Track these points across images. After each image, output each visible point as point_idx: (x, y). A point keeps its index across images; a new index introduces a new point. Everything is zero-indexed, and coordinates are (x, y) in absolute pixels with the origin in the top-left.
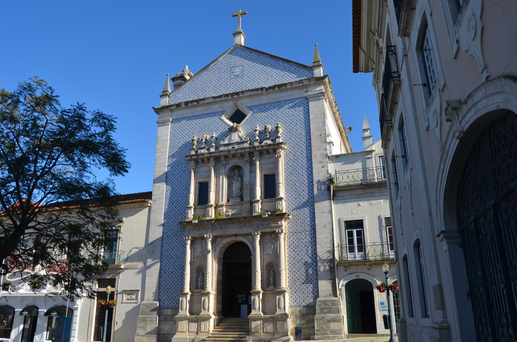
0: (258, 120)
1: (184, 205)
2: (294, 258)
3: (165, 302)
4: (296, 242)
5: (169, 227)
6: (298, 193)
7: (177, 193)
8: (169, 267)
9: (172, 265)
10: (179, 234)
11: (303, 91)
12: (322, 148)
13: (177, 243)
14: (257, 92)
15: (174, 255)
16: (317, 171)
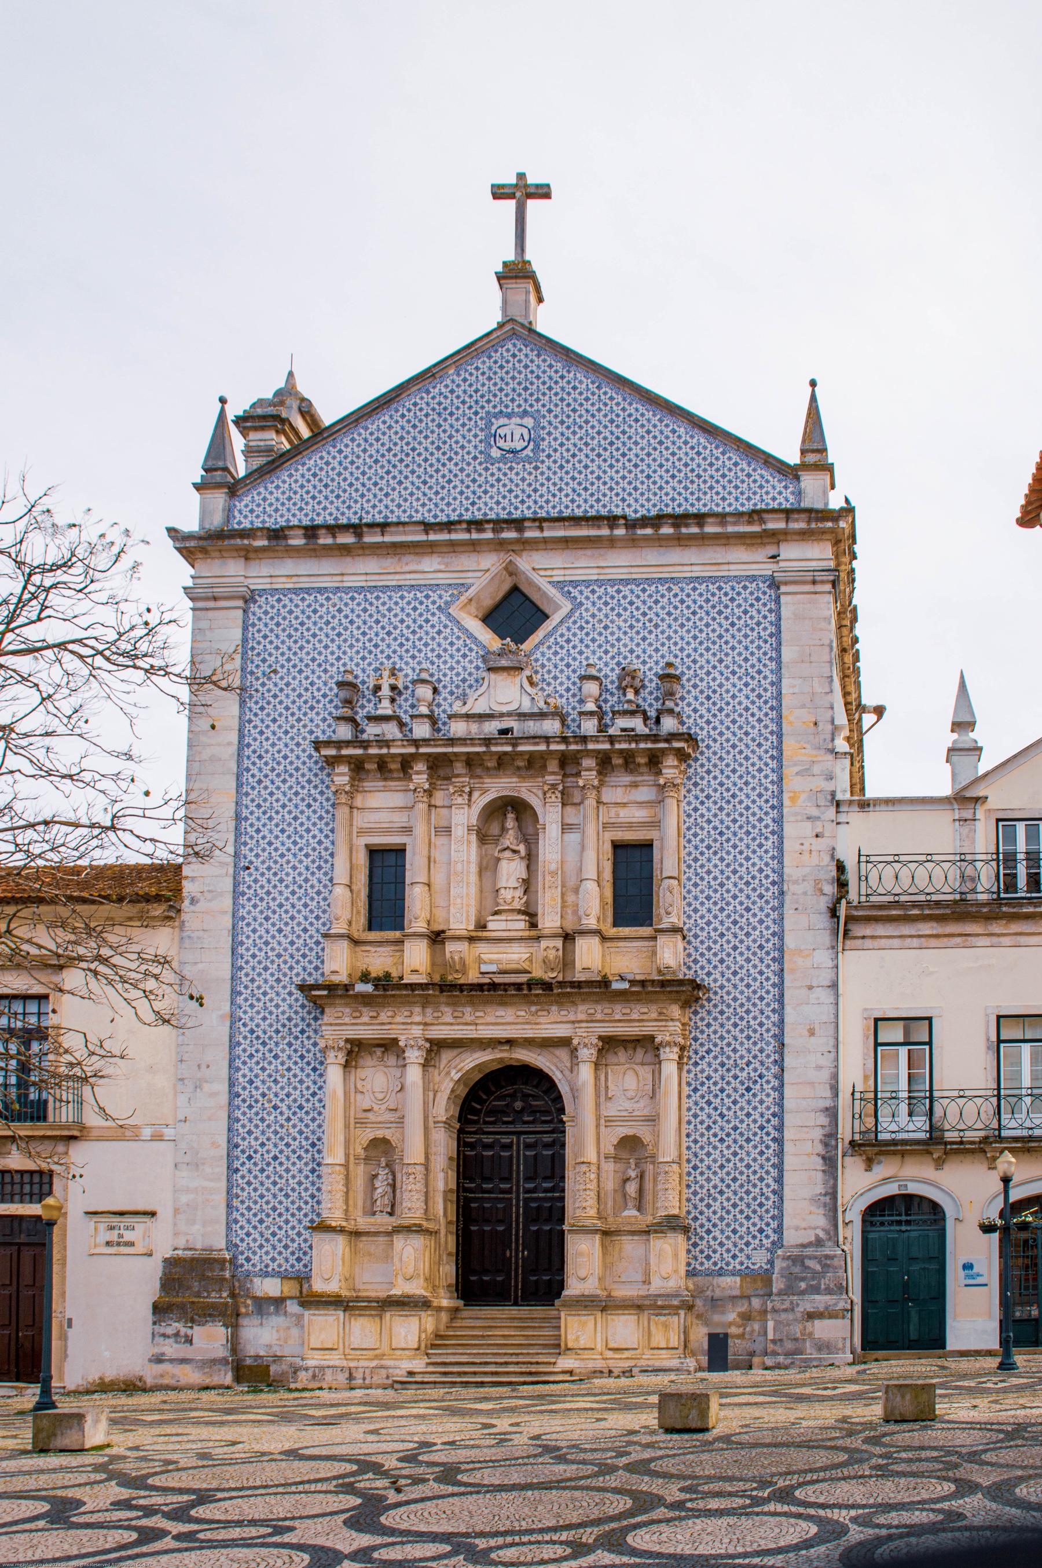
0: (593, 640)
1: (311, 924)
2: (709, 1128)
3: (255, 1253)
4: (716, 1077)
5: (259, 1000)
6: (729, 916)
7: (281, 881)
8: (263, 1139)
9: (276, 1132)
10: (296, 1026)
11: (761, 554)
12: (816, 769)
13: (289, 1057)
14: (605, 532)
15: (282, 1100)
16: (798, 847)
